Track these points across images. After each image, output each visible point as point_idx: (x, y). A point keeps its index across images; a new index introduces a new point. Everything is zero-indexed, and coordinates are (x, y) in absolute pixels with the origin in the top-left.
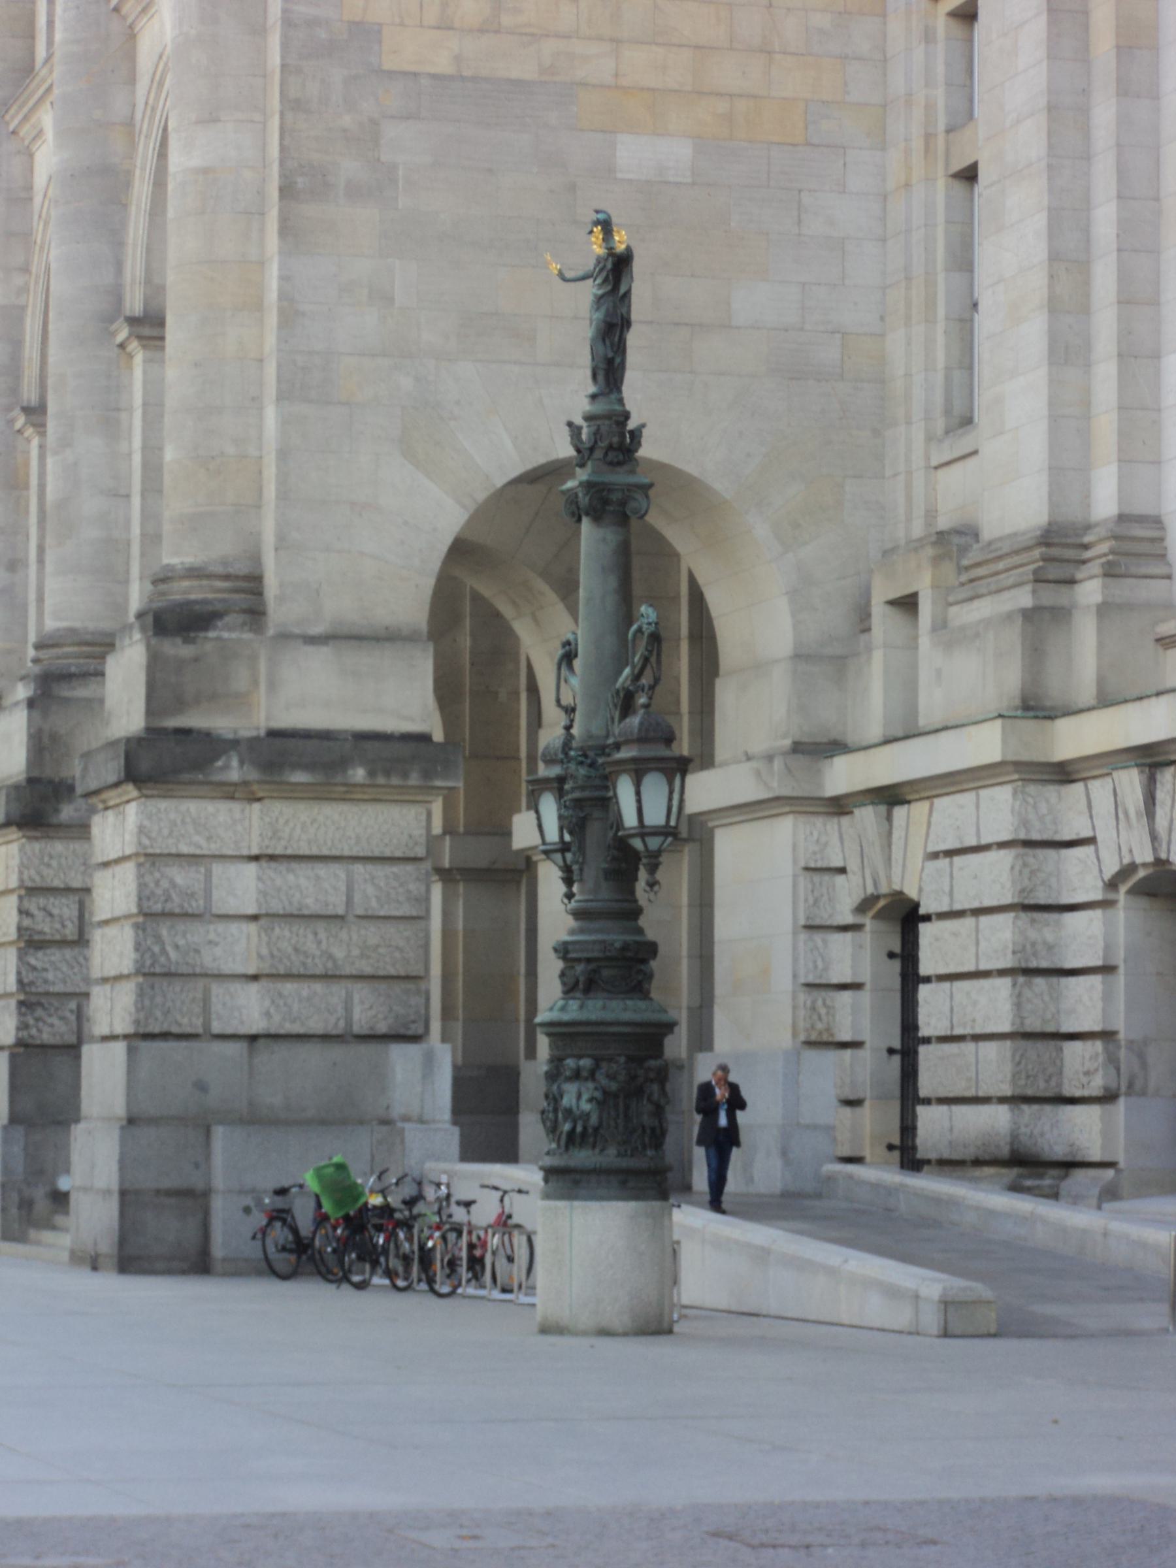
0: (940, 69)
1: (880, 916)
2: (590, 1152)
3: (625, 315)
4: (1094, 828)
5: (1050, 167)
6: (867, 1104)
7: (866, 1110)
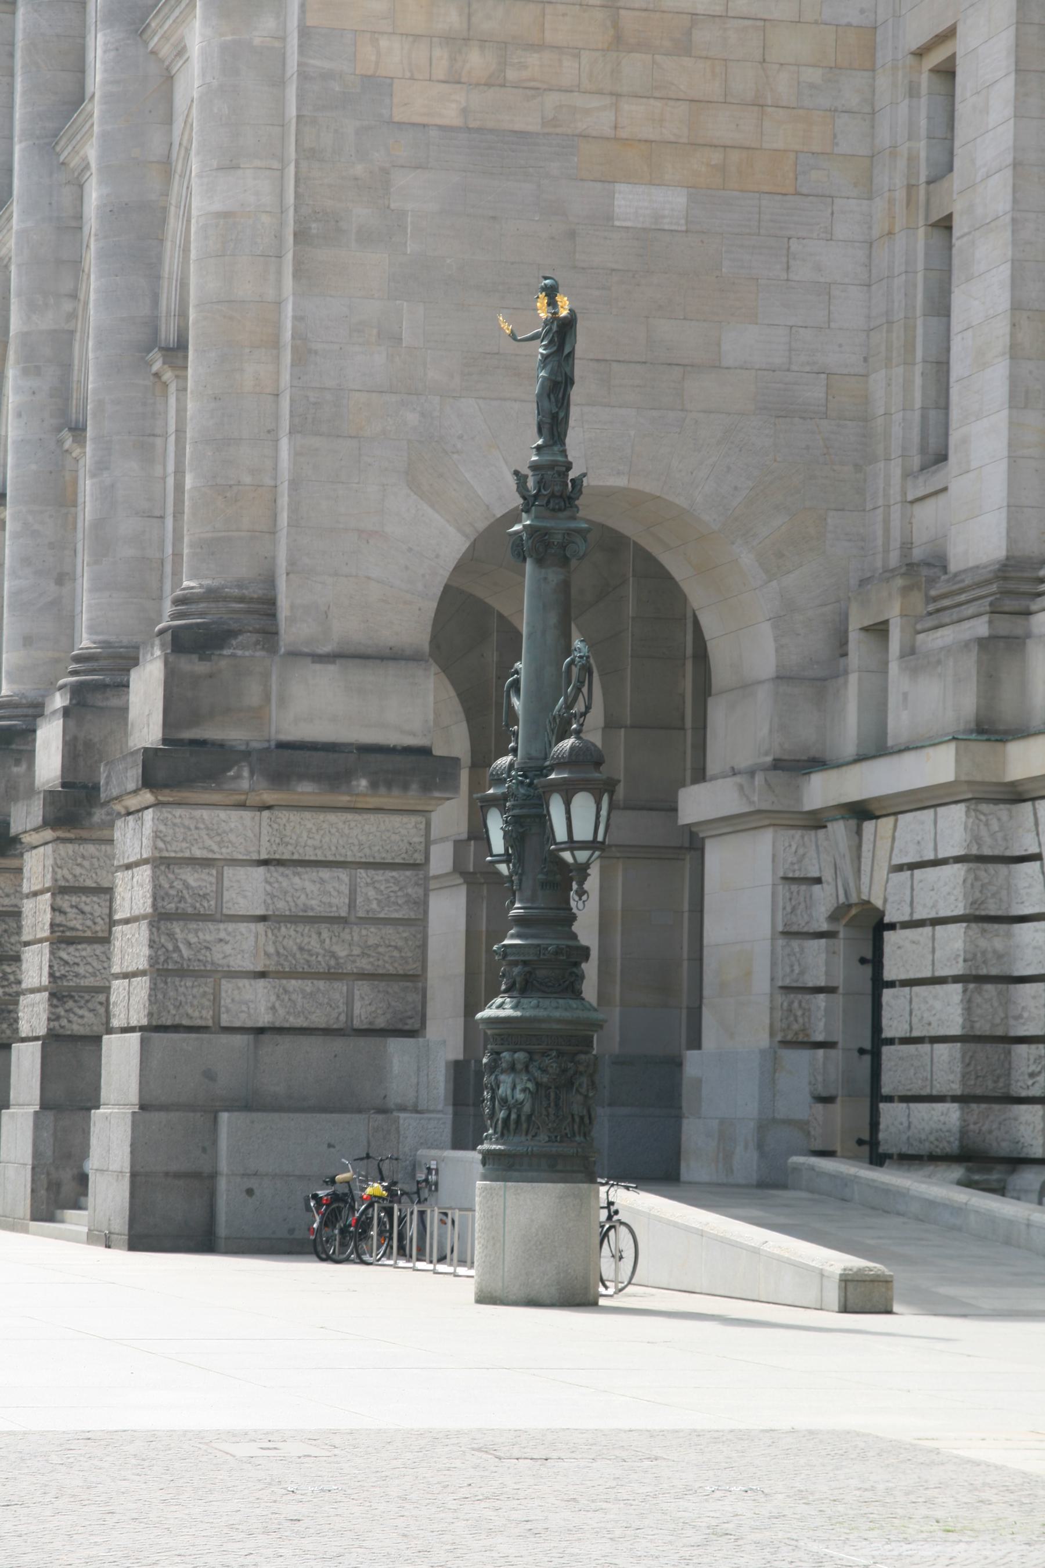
0: (923, 123)
2: (523, 1138)
3: (569, 374)
4: (1040, 845)
5: (1014, 221)
6: (839, 1099)
7: (837, 1107)
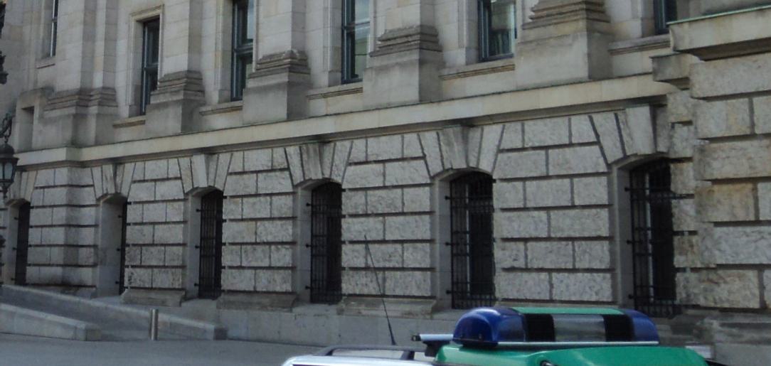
1: (14, 206)
